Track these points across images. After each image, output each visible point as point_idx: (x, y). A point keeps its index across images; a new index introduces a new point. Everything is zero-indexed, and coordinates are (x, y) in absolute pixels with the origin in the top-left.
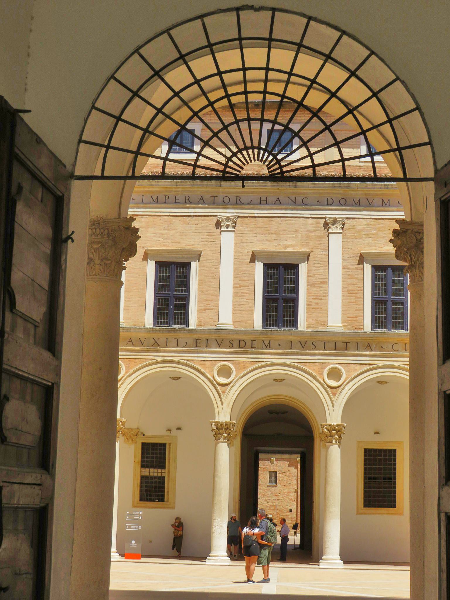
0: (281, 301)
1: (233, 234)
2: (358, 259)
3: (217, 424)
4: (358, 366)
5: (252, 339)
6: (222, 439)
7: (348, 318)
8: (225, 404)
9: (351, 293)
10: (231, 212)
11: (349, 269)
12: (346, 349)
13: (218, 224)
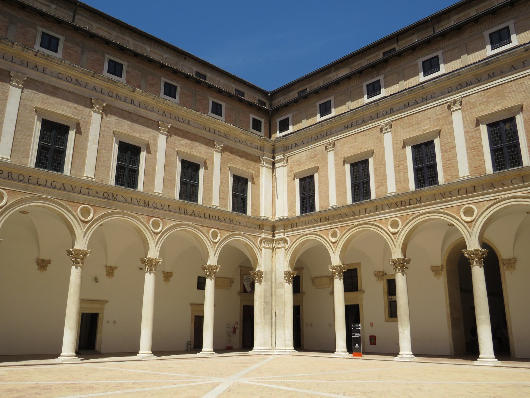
0: (426, 169)
1: (390, 133)
2: (475, 123)
3: (393, 261)
4: (486, 202)
5: (409, 199)
6: (397, 271)
8: (397, 247)
10: (388, 120)
11: (470, 132)
12: (475, 191)
13: (381, 130)
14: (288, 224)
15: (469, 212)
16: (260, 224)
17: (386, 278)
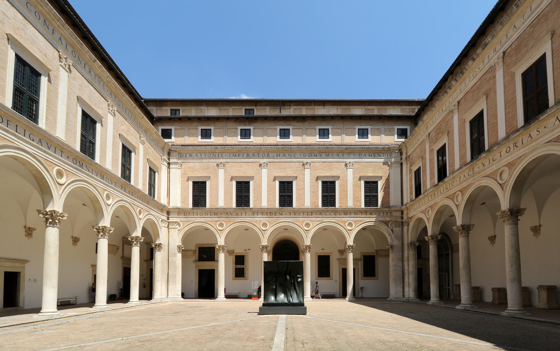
7: (312, 203)
9: (313, 192)
14: (181, 212)
15: (307, 225)
16: (161, 208)
17: (234, 255)
